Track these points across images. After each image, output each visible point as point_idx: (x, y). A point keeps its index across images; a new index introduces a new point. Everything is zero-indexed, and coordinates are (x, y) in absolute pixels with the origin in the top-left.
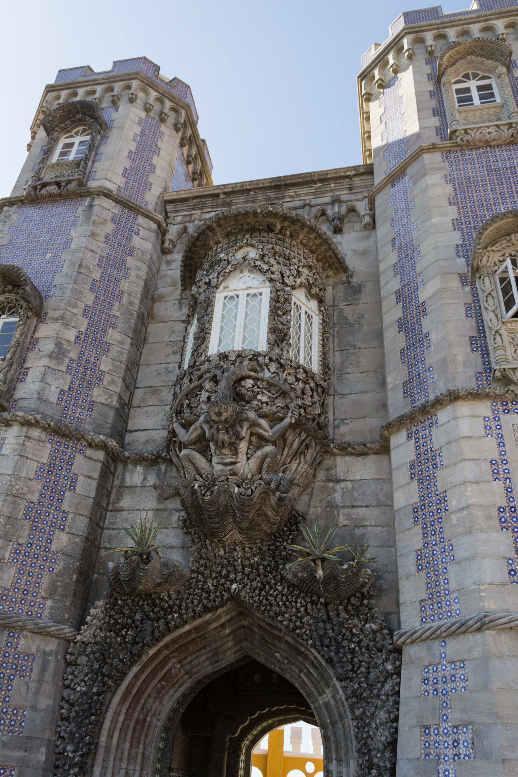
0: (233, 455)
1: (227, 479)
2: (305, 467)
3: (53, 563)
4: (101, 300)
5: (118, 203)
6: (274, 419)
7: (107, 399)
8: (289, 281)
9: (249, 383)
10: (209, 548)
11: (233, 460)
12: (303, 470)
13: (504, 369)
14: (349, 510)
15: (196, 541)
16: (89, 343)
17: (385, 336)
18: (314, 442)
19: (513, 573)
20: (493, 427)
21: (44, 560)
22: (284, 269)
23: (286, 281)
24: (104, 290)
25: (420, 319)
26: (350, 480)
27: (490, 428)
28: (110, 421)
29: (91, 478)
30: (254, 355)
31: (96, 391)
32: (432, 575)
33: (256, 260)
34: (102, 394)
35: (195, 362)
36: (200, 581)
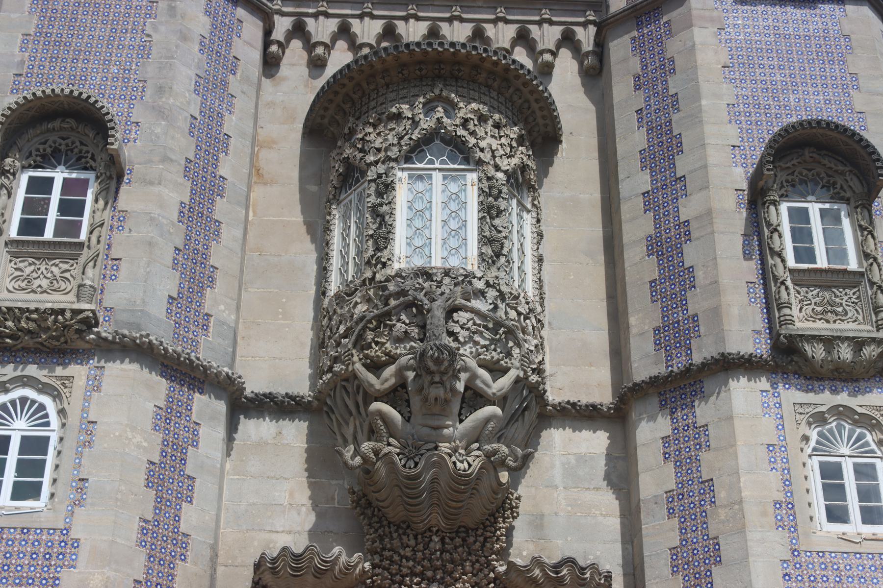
1: (436, 448)
3: (184, 548)
4: (203, 150)
8: (504, 164)
9: (462, 316)
10: (395, 535)
13: (791, 335)
15: (377, 525)
16: (195, 221)
17: (626, 256)
18: (534, 403)
19: (787, 578)
20: (772, 404)
21: (175, 545)
22: (495, 144)
24: (205, 133)
25: (681, 244)
27: (768, 406)
30: (466, 276)
32: (692, 578)
33: (456, 125)
35: (374, 273)
36: (387, 579)
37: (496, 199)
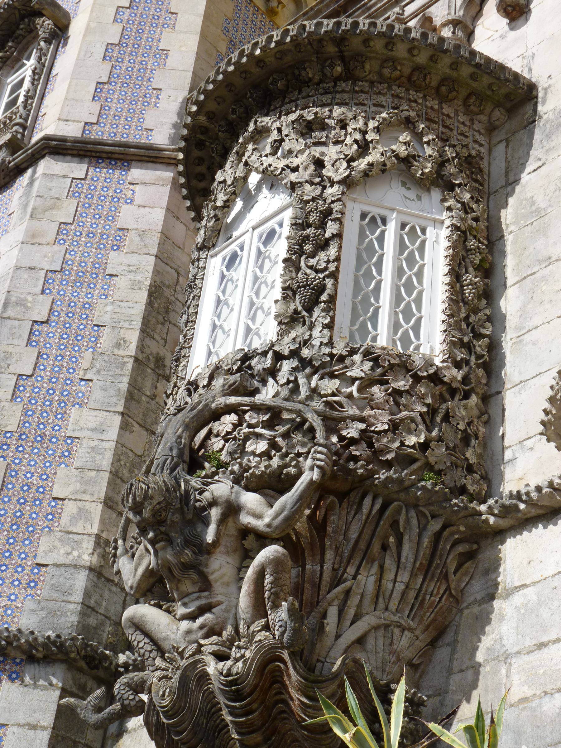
0: (201, 590)
2: (404, 577)
4: (52, 357)
5: (85, 156)
6: (273, 485)
7: (68, 554)
11: (203, 602)
12: (400, 587)
14: (532, 657)
16: (28, 450)
23: (330, 174)
26: (534, 583)
28: (78, 597)
29: (34, 727)
31: (45, 542)
34: (58, 545)
37: (322, 225)
